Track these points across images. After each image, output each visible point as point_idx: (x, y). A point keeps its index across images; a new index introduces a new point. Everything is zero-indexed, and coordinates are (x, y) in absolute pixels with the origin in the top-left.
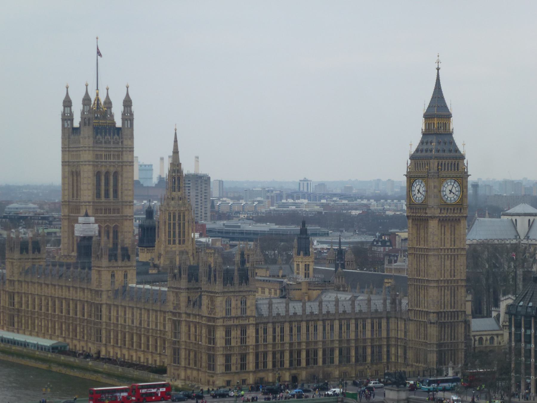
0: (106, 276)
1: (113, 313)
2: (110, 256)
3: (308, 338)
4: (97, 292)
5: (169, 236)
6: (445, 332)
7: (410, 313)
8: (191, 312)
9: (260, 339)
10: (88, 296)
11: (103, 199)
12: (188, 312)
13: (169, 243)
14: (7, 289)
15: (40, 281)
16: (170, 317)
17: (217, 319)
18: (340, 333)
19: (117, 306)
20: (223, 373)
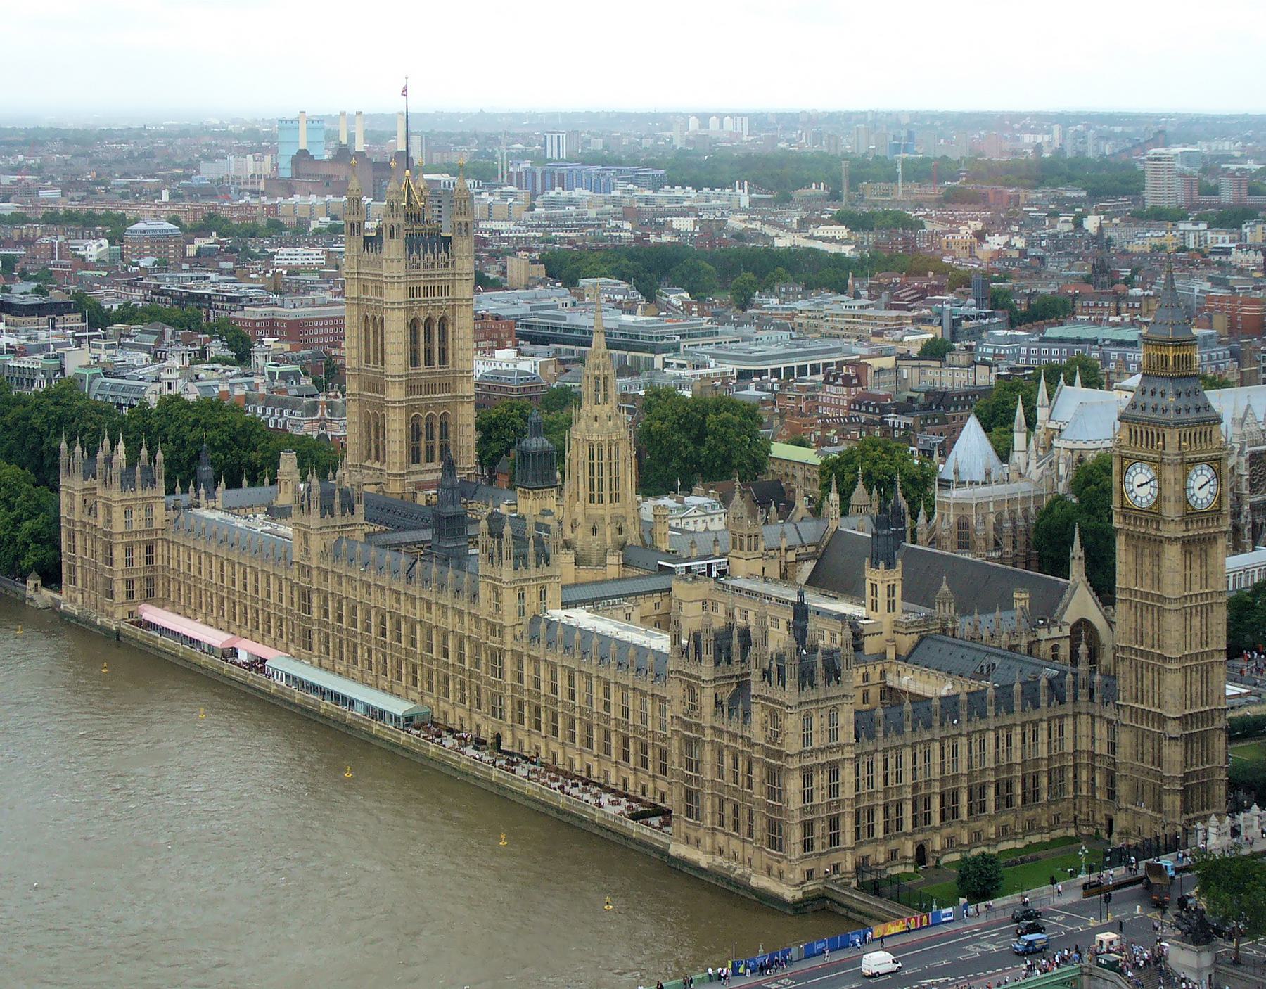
0: (509, 599)
1: (528, 671)
2: (516, 557)
3: (942, 772)
4: (494, 625)
5: (592, 488)
6: (1192, 752)
7: (1121, 712)
8: (721, 726)
9: (861, 783)
10: (468, 627)
11: (422, 368)
12: (716, 725)
13: (592, 500)
14: (296, 581)
15: (363, 578)
16: (677, 728)
17: (788, 755)
18: (997, 753)
19: (536, 661)
20: (801, 858)
